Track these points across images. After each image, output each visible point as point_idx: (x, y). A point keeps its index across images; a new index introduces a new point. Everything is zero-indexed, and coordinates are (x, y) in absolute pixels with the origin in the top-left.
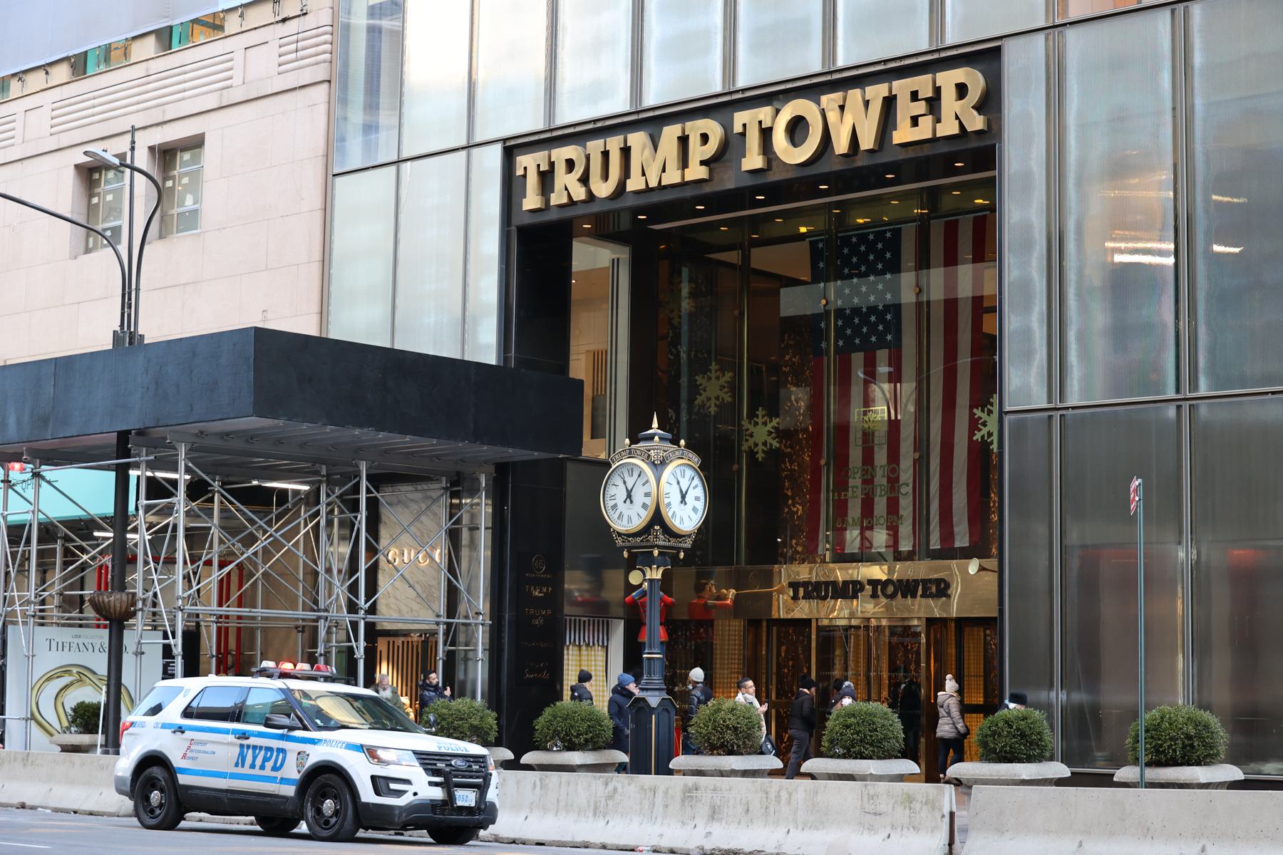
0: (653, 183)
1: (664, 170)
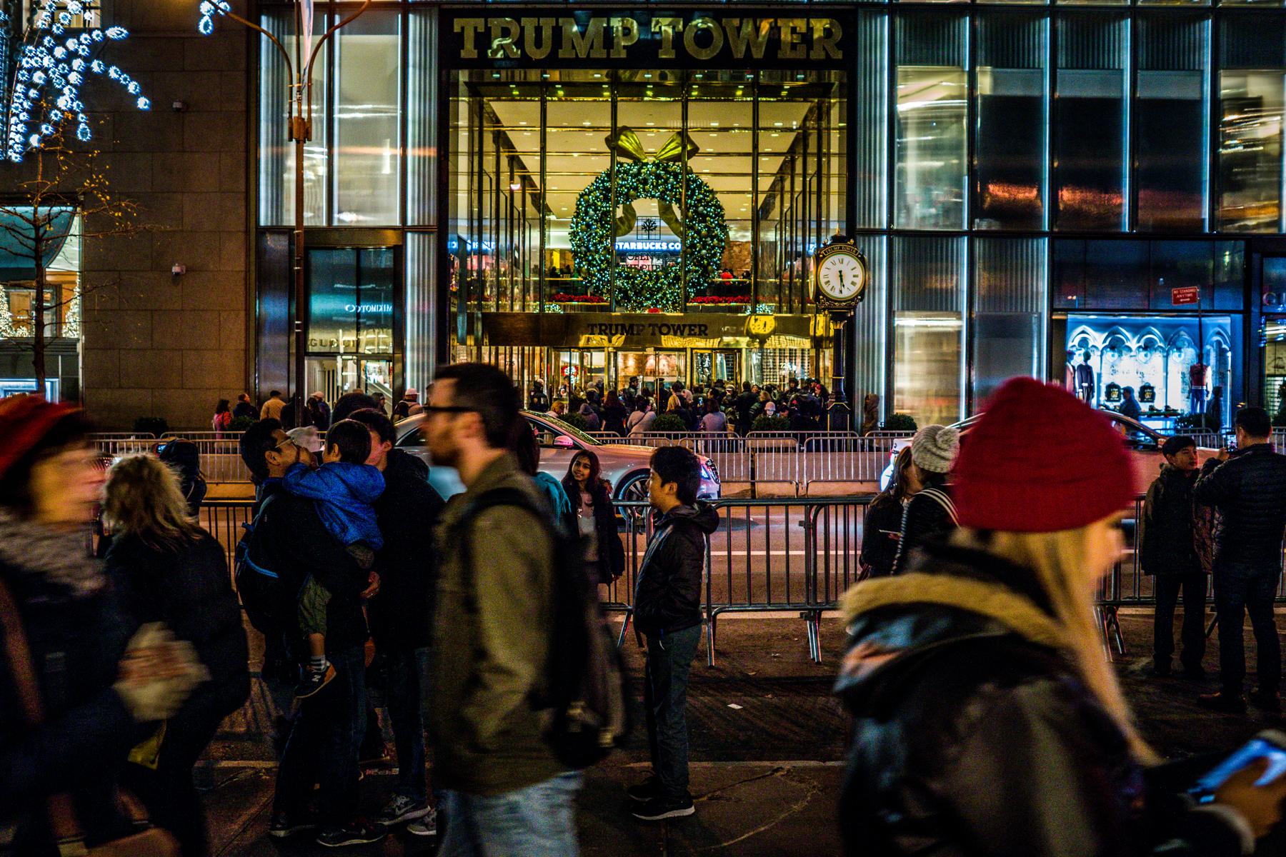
0: (582, 55)
1: (592, 47)
